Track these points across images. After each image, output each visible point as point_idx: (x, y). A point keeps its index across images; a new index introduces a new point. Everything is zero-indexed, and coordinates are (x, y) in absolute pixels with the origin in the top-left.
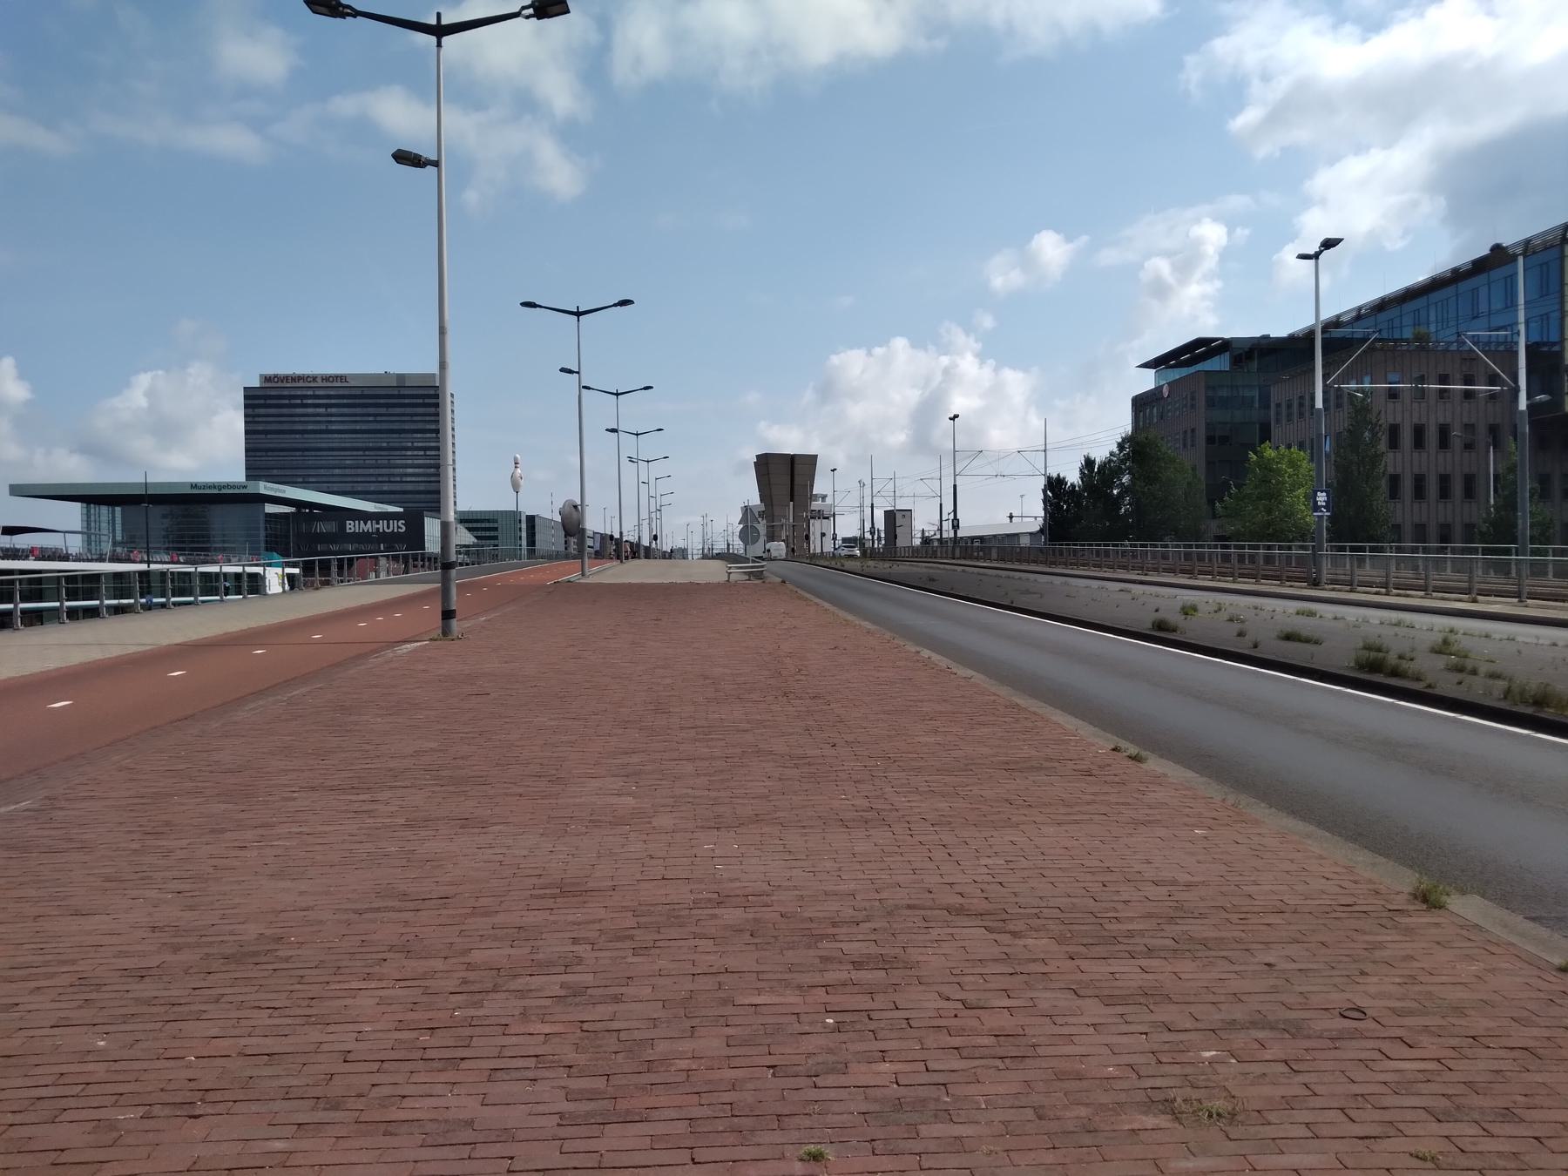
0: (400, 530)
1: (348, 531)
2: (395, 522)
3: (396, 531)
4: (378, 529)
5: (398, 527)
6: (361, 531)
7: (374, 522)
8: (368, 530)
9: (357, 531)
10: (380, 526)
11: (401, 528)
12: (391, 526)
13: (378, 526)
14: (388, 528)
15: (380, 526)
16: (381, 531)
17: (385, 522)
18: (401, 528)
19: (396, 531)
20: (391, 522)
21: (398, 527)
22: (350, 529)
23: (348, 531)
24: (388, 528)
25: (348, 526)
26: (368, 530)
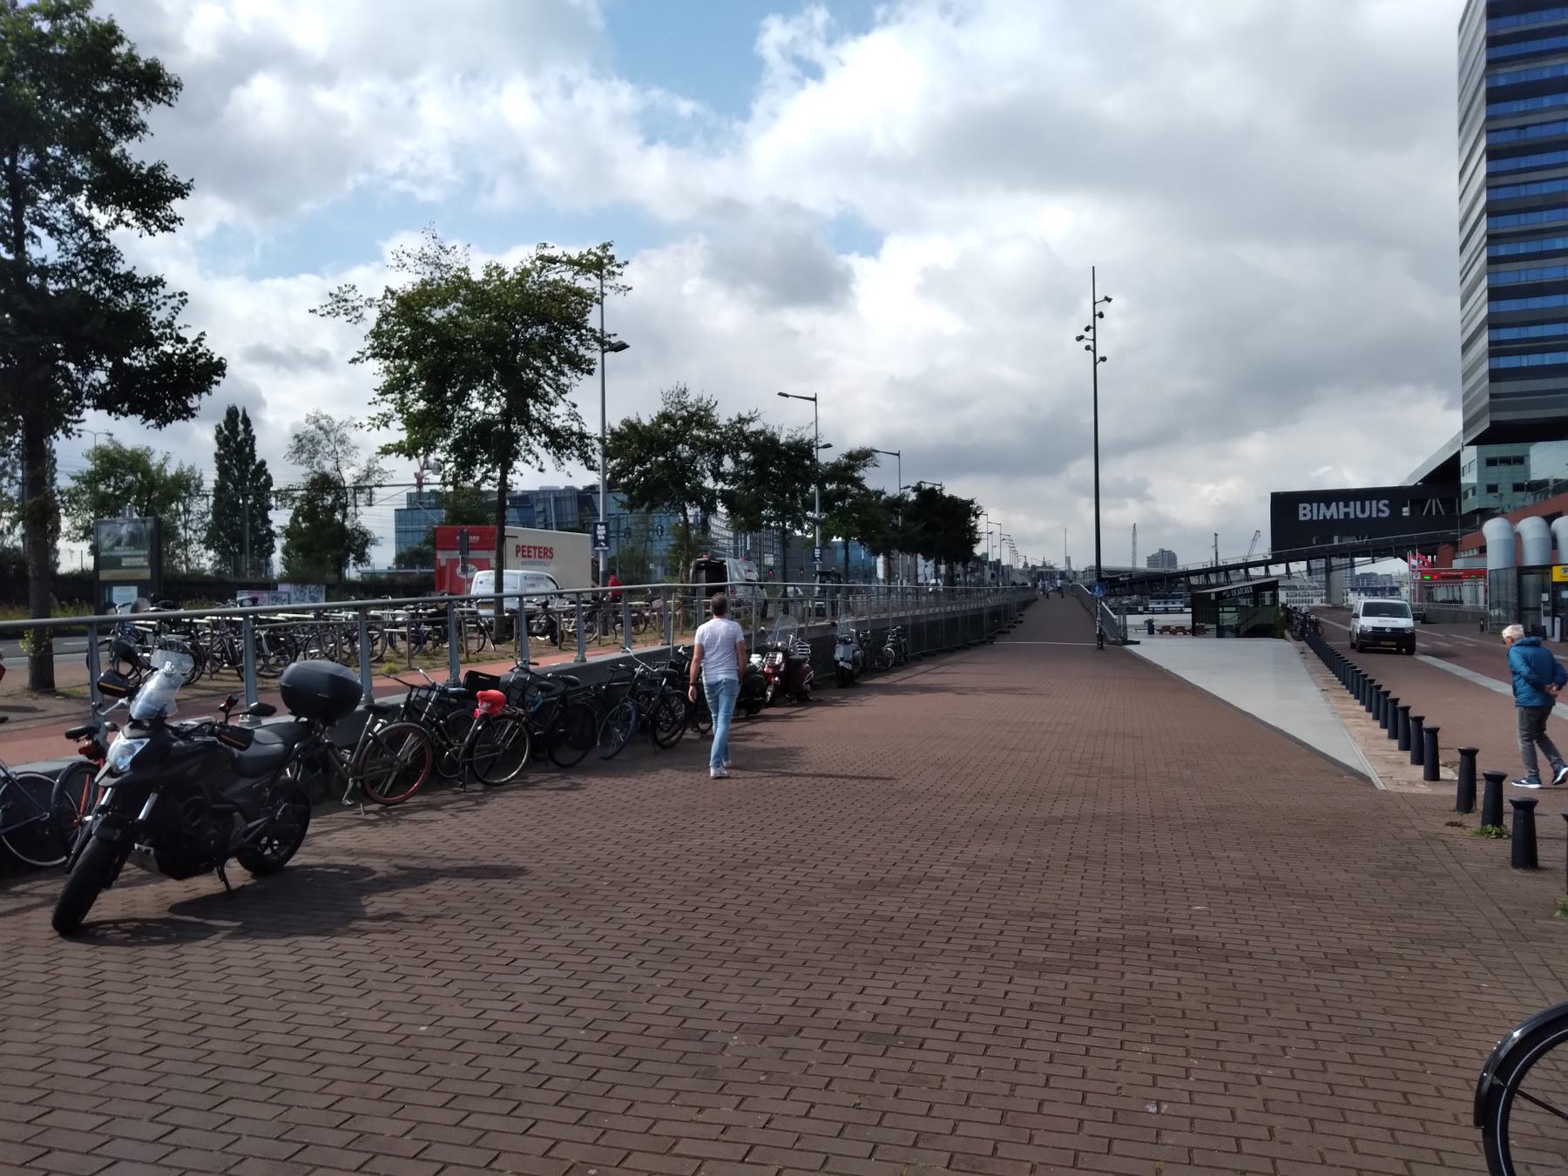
0: (1381, 515)
1: (1301, 518)
2: (1374, 502)
3: (1374, 515)
4: (1347, 514)
5: (1379, 510)
6: (1321, 518)
7: (1341, 504)
8: (1332, 516)
9: (1315, 518)
10: (1351, 510)
11: (1383, 512)
12: (1367, 509)
13: (1347, 510)
14: (1363, 511)
15: (1351, 510)
16: (1352, 516)
17: (1358, 503)
18: (1383, 512)
19: (1374, 515)
20: (1367, 503)
21: (1379, 510)
22: (1305, 515)
23: (1301, 518)
24: (1363, 511)
25: (1301, 512)
26: (1332, 516)
